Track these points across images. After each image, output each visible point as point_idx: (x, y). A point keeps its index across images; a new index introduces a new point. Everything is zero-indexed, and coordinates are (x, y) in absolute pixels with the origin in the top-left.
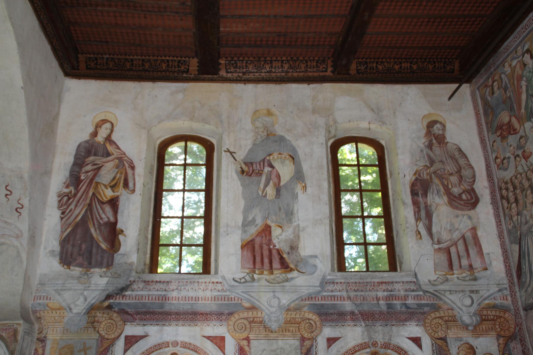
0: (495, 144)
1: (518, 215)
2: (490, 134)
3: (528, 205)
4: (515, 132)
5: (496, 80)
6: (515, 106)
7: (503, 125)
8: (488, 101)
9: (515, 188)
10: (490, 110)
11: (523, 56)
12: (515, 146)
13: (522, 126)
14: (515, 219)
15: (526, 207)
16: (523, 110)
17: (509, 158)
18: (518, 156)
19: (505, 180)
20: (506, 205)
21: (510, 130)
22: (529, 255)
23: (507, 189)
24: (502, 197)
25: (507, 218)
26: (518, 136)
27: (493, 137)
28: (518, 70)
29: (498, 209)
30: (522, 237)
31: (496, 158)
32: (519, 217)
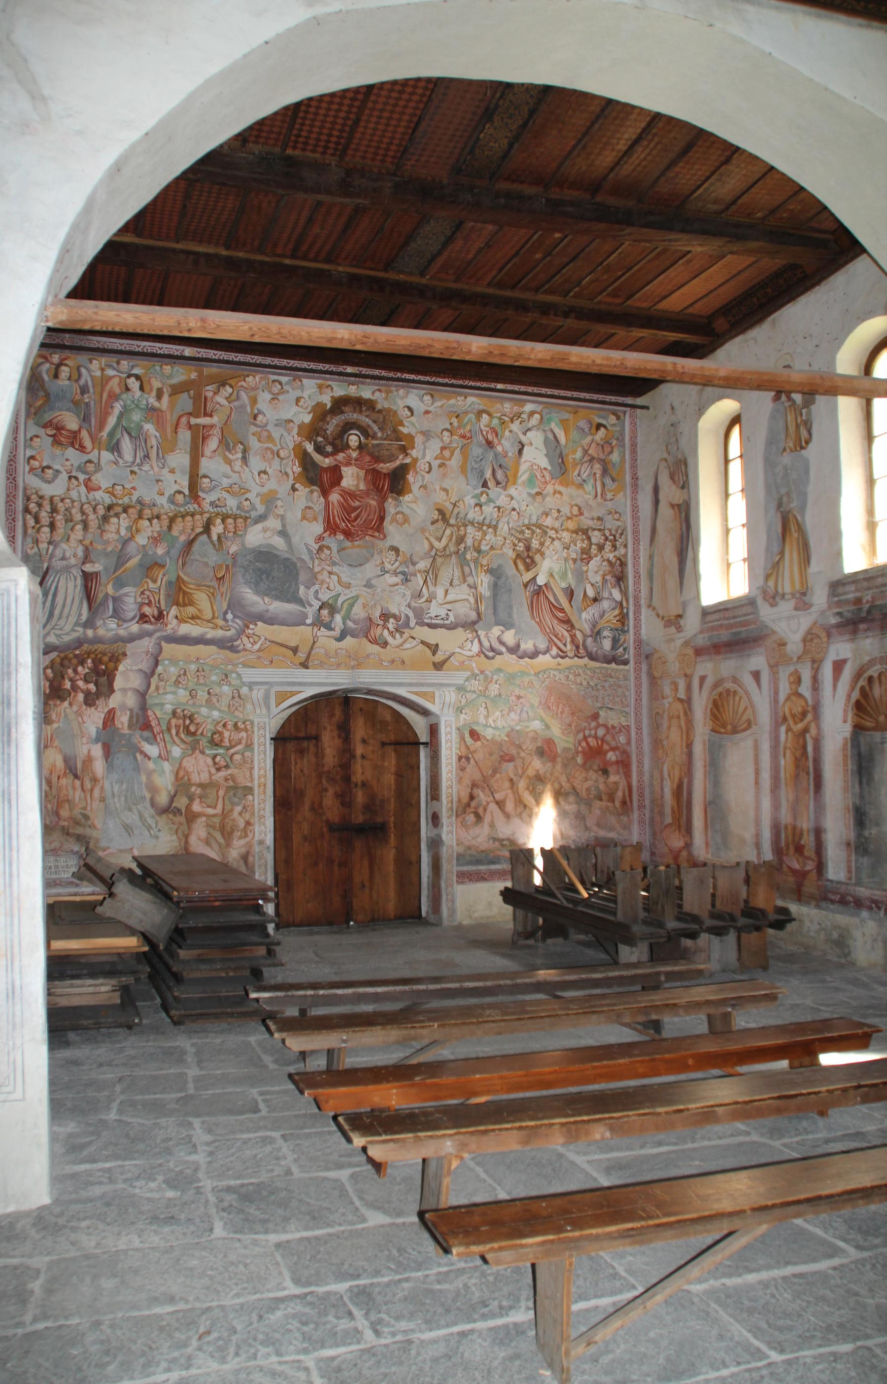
0: (35, 439)
1: (50, 543)
2: (31, 422)
3: (72, 539)
4: (82, 449)
5: (66, 365)
6: (93, 420)
7: (63, 428)
8: (43, 380)
9: (54, 510)
10: (42, 393)
11: (129, 376)
12: (76, 464)
13: (96, 451)
14: (43, 546)
15: (68, 540)
16: (104, 434)
17: (58, 471)
18: (77, 478)
19: (40, 493)
20: (31, 522)
21: (74, 440)
22: (55, 595)
23: (40, 505)
24: (26, 510)
25: (29, 540)
26: (86, 457)
27: (33, 430)
28: (114, 385)
29: (13, 520)
30: (50, 572)
31: (32, 457)
32: (51, 547)
